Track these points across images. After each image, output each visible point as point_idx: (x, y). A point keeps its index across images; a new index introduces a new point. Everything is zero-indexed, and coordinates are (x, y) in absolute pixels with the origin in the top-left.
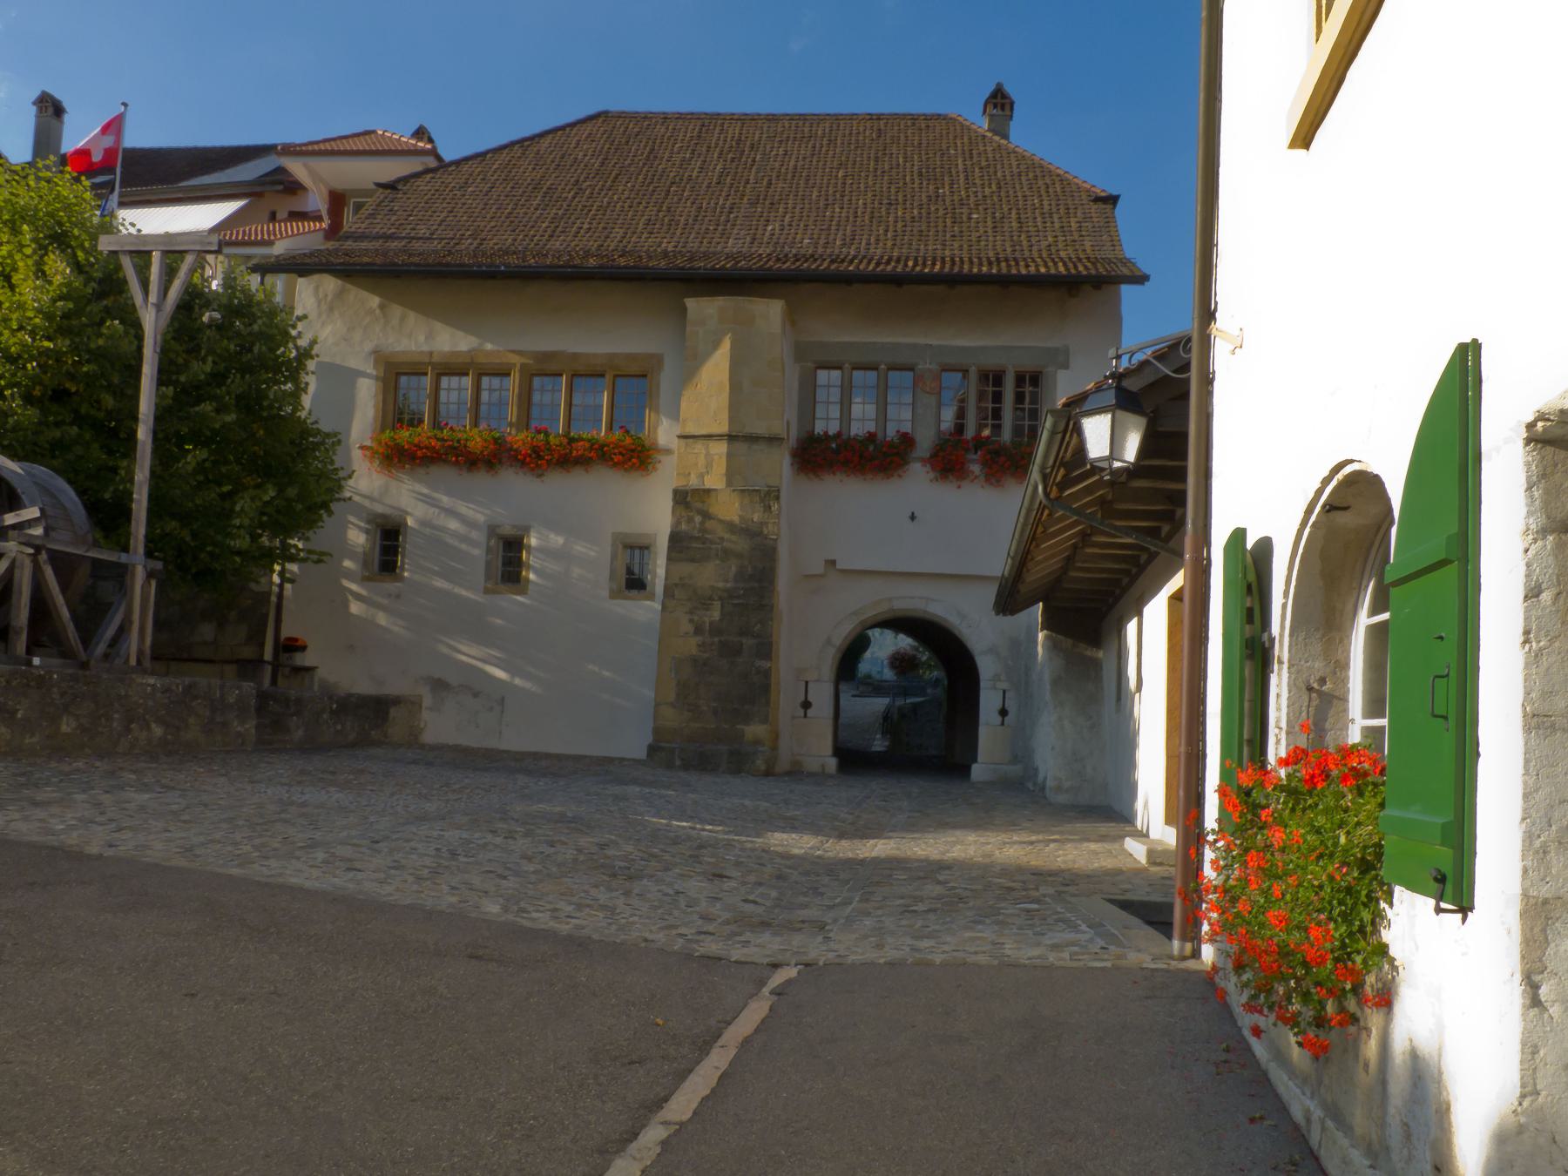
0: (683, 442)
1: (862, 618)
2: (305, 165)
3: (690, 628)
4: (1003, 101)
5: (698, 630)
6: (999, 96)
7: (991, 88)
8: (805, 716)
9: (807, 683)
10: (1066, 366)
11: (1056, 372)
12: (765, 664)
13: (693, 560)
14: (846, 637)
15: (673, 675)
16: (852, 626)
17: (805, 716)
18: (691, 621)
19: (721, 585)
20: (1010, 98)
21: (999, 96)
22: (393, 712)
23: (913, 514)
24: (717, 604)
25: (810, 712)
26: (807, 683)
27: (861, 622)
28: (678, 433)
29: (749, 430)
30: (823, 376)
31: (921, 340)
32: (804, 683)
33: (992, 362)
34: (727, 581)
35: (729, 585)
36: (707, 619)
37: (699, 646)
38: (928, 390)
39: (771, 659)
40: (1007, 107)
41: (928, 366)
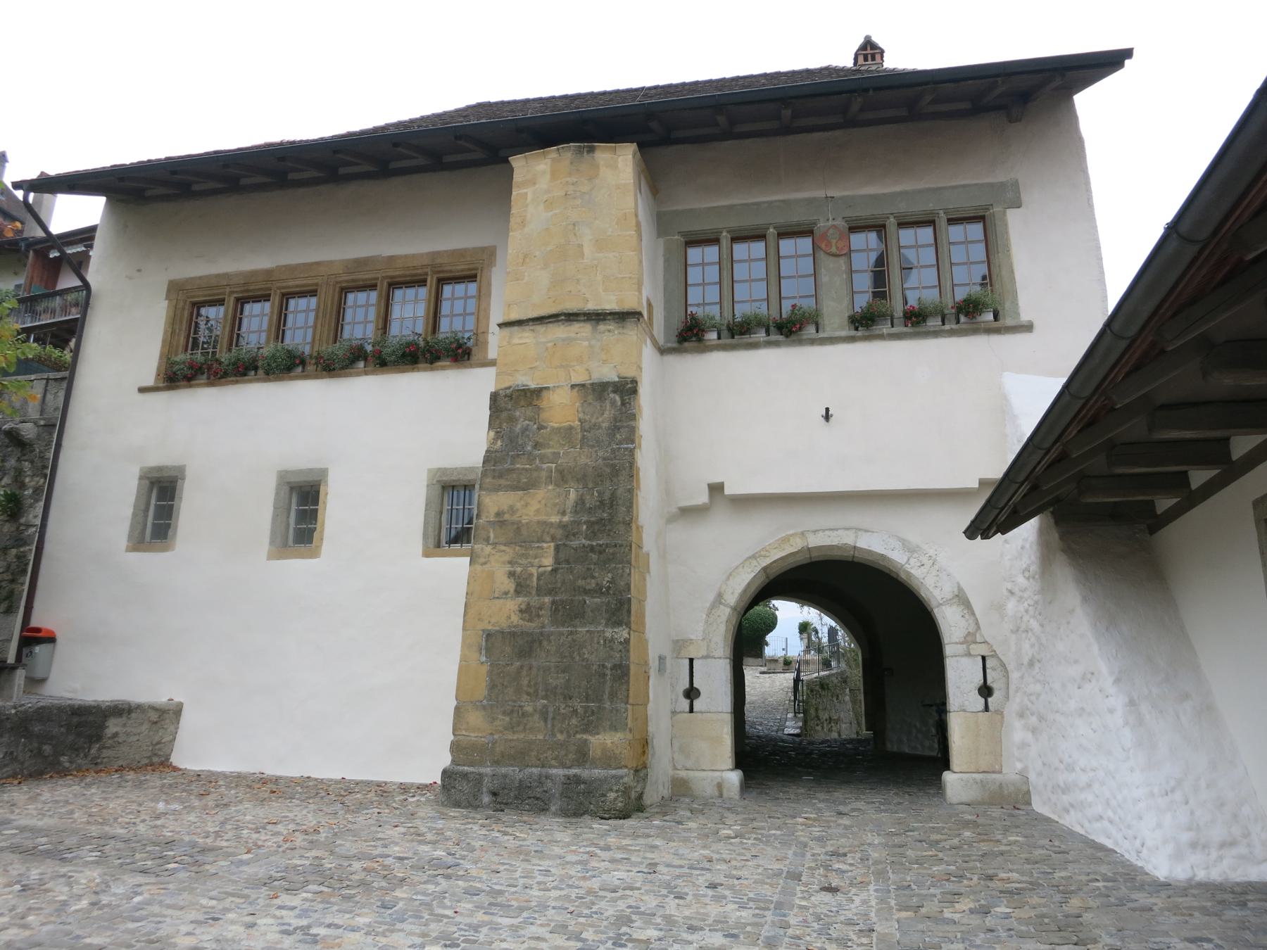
0: (507, 331)
3: (510, 585)
4: (872, 52)
5: (521, 588)
6: (869, 48)
7: (861, 41)
10: (1017, 204)
11: (1004, 214)
12: (623, 633)
13: (515, 488)
14: (745, 591)
15: (484, 659)
16: (753, 575)
18: (511, 574)
19: (555, 519)
20: (880, 48)
21: (869, 48)
22: (113, 726)
23: (827, 410)
24: (549, 547)
27: (765, 569)
28: (501, 321)
29: (591, 306)
30: (694, 254)
31: (820, 194)
34: (564, 513)
35: (566, 519)
36: (534, 571)
37: (521, 611)
38: (834, 250)
39: (628, 625)
40: (878, 57)
41: (830, 223)
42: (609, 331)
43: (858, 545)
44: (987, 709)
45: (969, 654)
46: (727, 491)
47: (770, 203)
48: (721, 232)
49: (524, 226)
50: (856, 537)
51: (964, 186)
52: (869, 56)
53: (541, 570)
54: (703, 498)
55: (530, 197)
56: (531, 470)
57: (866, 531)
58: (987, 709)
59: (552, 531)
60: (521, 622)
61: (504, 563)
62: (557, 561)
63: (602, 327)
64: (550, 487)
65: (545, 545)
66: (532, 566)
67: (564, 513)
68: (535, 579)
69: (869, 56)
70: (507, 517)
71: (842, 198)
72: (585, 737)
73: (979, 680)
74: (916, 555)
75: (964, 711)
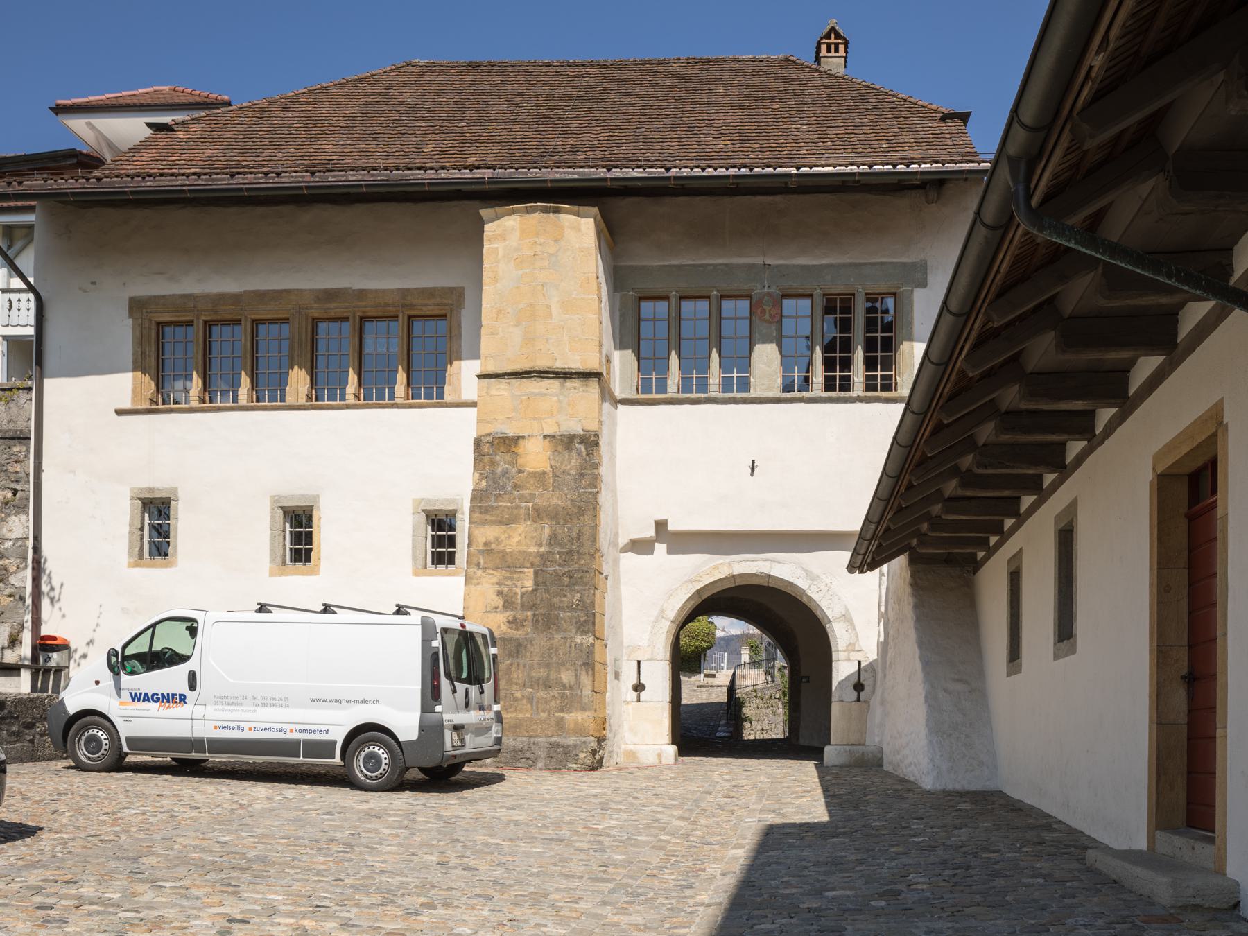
3: (499, 602)
4: (836, 41)
5: (508, 604)
6: (833, 36)
9: (639, 662)
11: (912, 291)
14: (682, 608)
18: (499, 593)
19: (533, 549)
21: (833, 36)
23: (753, 462)
24: (530, 572)
26: (639, 662)
27: (698, 592)
28: (479, 372)
29: (559, 365)
30: (647, 307)
31: (759, 261)
33: (838, 287)
34: (540, 545)
35: (542, 549)
36: (518, 591)
41: (766, 290)
42: (575, 388)
43: (772, 574)
44: (858, 700)
46: (670, 527)
47: (715, 266)
48: (671, 292)
49: (497, 281)
50: (771, 568)
51: (882, 263)
52: (833, 46)
53: (523, 590)
54: (650, 532)
55: (501, 253)
56: (512, 508)
57: (779, 562)
58: (858, 700)
59: (531, 559)
60: (509, 630)
61: (493, 584)
62: (536, 583)
63: (568, 384)
64: (529, 523)
65: (526, 570)
66: (516, 587)
67: (540, 545)
68: (519, 597)
69: (833, 46)
70: (493, 546)
71: (777, 266)
72: (562, 715)
74: (815, 583)
75: (842, 701)
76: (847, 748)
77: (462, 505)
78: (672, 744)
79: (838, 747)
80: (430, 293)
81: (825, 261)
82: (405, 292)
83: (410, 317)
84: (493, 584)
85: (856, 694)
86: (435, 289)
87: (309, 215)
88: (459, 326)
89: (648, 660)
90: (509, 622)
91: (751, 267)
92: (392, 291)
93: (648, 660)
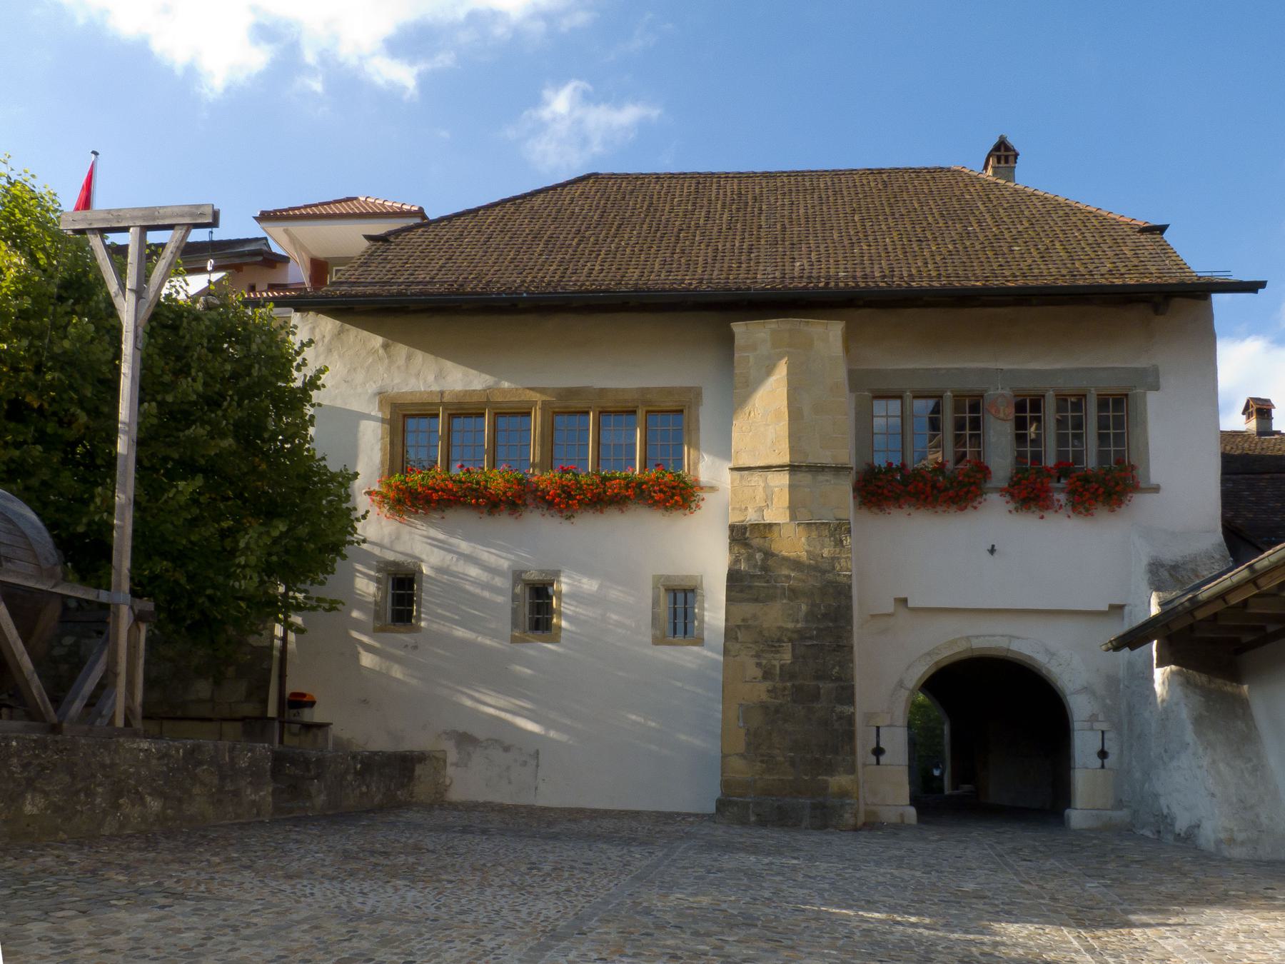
0: (737, 474)
1: (937, 658)
2: (286, 231)
3: (758, 673)
5: (767, 675)
6: (1003, 149)
7: (995, 140)
8: (878, 763)
9: (878, 728)
10: (1156, 387)
11: (1145, 394)
12: (847, 709)
13: (756, 600)
15: (741, 725)
17: (878, 763)
18: (758, 665)
19: (790, 626)
20: (1014, 150)
21: (1003, 149)
22: (419, 769)
23: (993, 546)
25: (883, 759)
26: (878, 728)
29: (812, 460)
30: (879, 407)
31: (992, 365)
32: (875, 729)
33: (1070, 385)
35: (799, 625)
36: (776, 663)
37: (768, 691)
38: (1002, 415)
40: (1011, 159)
41: (1000, 391)
42: (827, 481)
43: (1011, 648)
44: (1103, 767)
45: (1092, 729)
46: (910, 604)
47: (948, 370)
48: (906, 392)
49: (748, 386)
50: (1010, 642)
51: (1113, 369)
52: (1003, 158)
53: (782, 662)
54: (890, 608)
55: (751, 360)
56: (768, 587)
57: (1018, 638)
58: (1103, 767)
59: (789, 634)
60: (769, 700)
61: (752, 656)
62: (794, 656)
63: (821, 478)
64: (785, 601)
65: (784, 644)
66: (775, 660)
67: (797, 621)
68: (778, 669)
69: (1003, 158)
70: (750, 622)
71: (1011, 371)
73: (1098, 747)
74: (1055, 657)
75: (1087, 768)
76: (1094, 812)
77: (702, 582)
78: (911, 805)
79: (1085, 812)
80: (669, 391)
81: (1058, 366)
82: (644, 391)
83: (647, 412)
84: (752, 656)
85: (1100, 761)
86: (673, 388)
87: (926, 394)
88: (698, 421)
89: (888, 726)
90: (768, 691)
91: (984, 371)
92: (631, 390)
93: (888, 726)
